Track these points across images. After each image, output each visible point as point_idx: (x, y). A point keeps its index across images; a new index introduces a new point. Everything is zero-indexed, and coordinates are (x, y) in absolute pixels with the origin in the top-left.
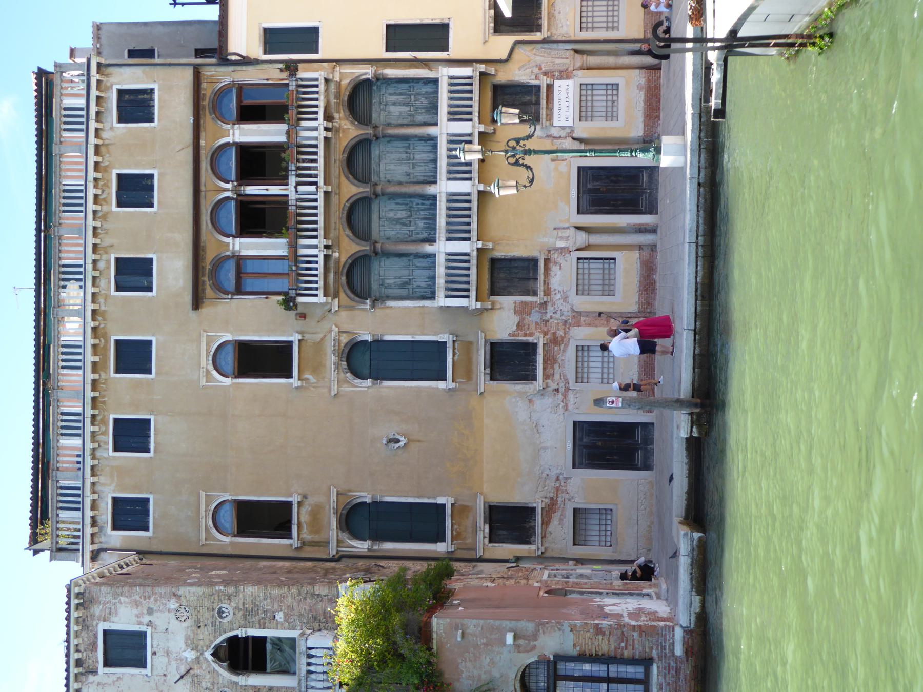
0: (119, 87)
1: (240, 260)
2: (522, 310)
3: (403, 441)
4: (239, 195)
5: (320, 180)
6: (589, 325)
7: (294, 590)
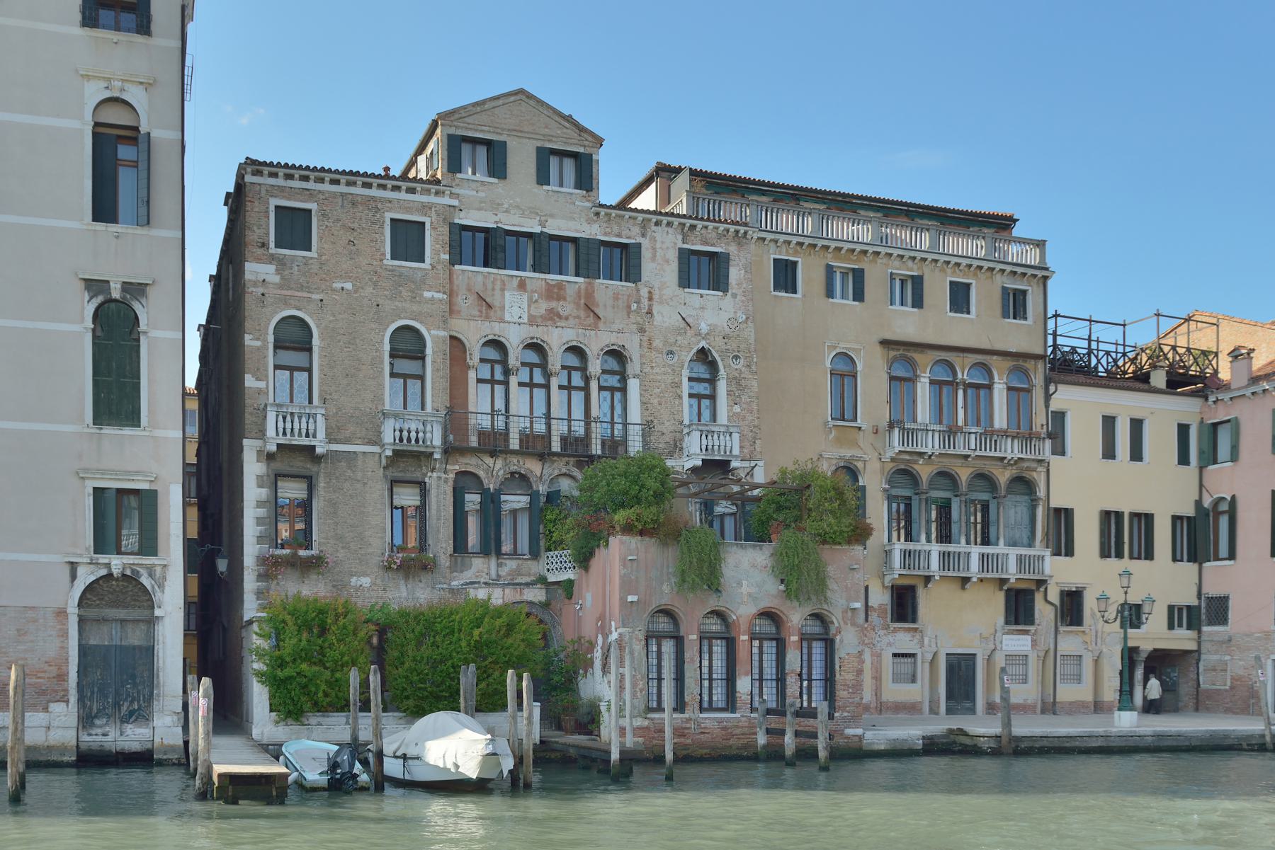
1: (912, 380)
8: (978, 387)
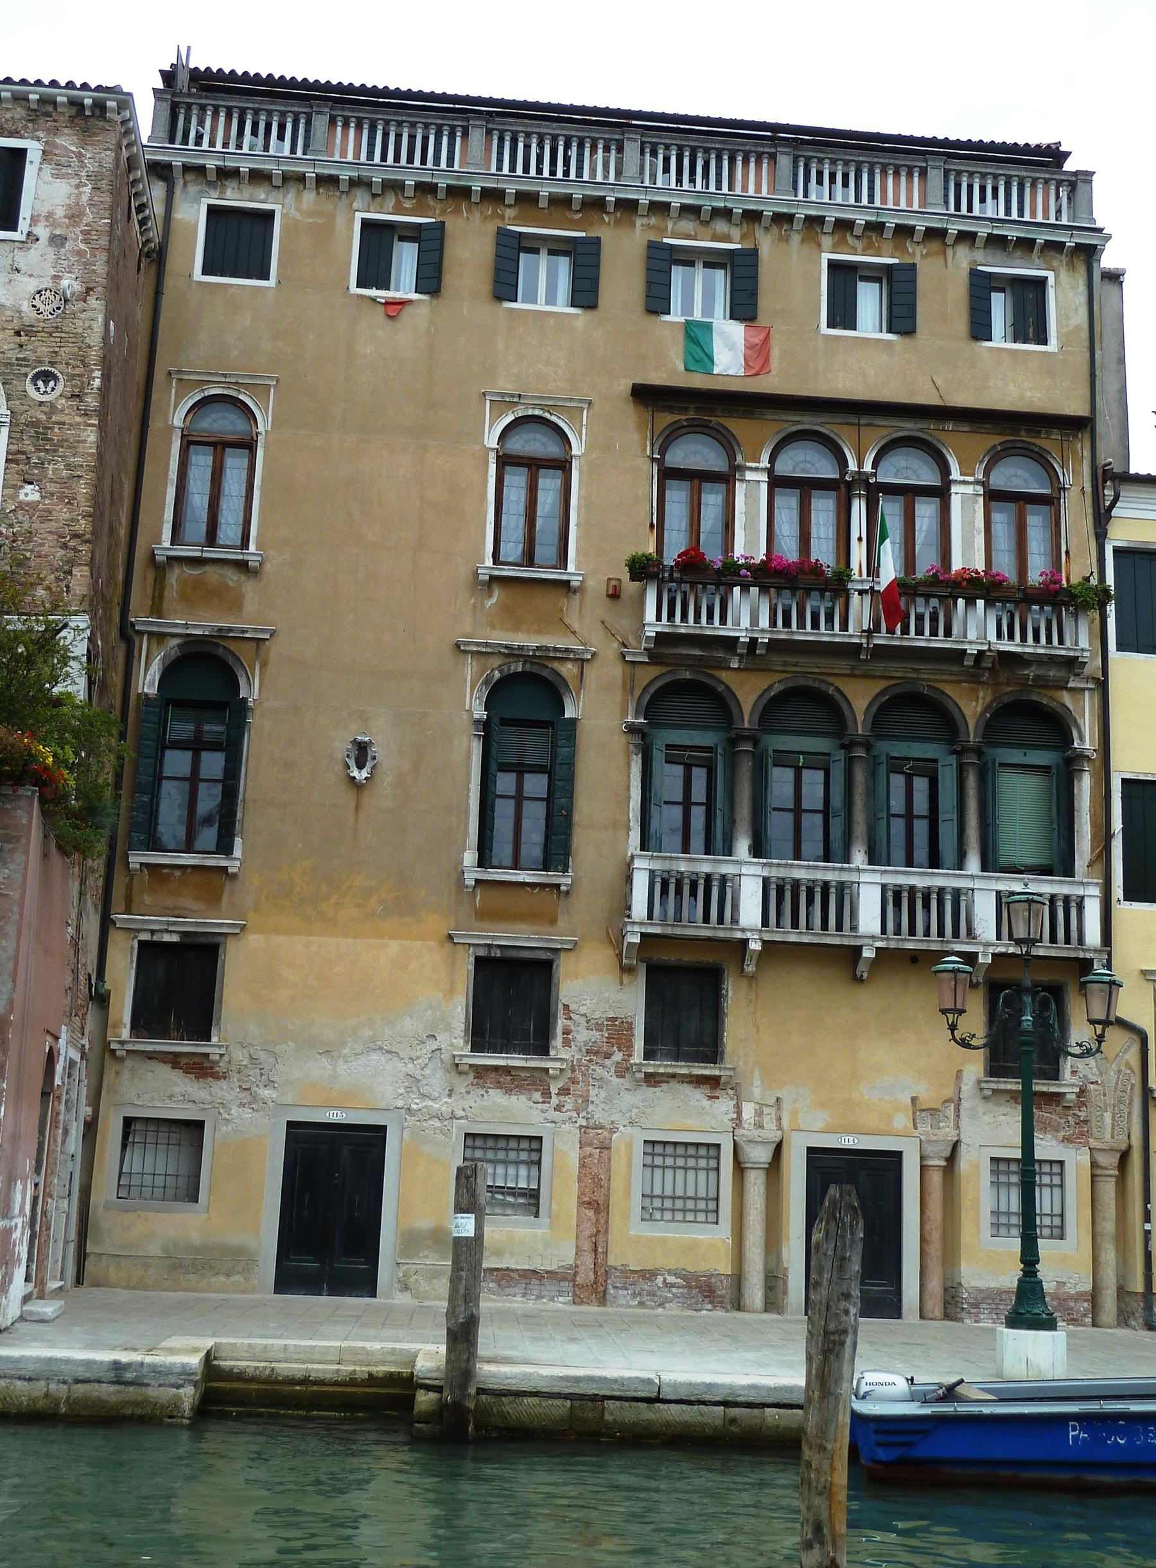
0: (1051, 281)
2: (618, 1032)
3: (361, 775)
4: (849, 486)
6: (583, 1165)
7: (83, 525)
8: (909, 493)
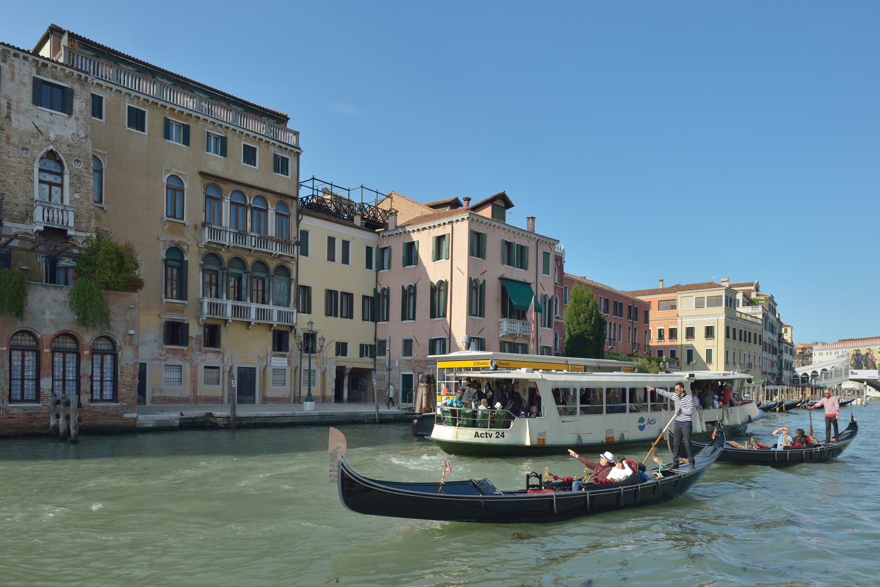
1: (220, 200)
5: (256, 248)
